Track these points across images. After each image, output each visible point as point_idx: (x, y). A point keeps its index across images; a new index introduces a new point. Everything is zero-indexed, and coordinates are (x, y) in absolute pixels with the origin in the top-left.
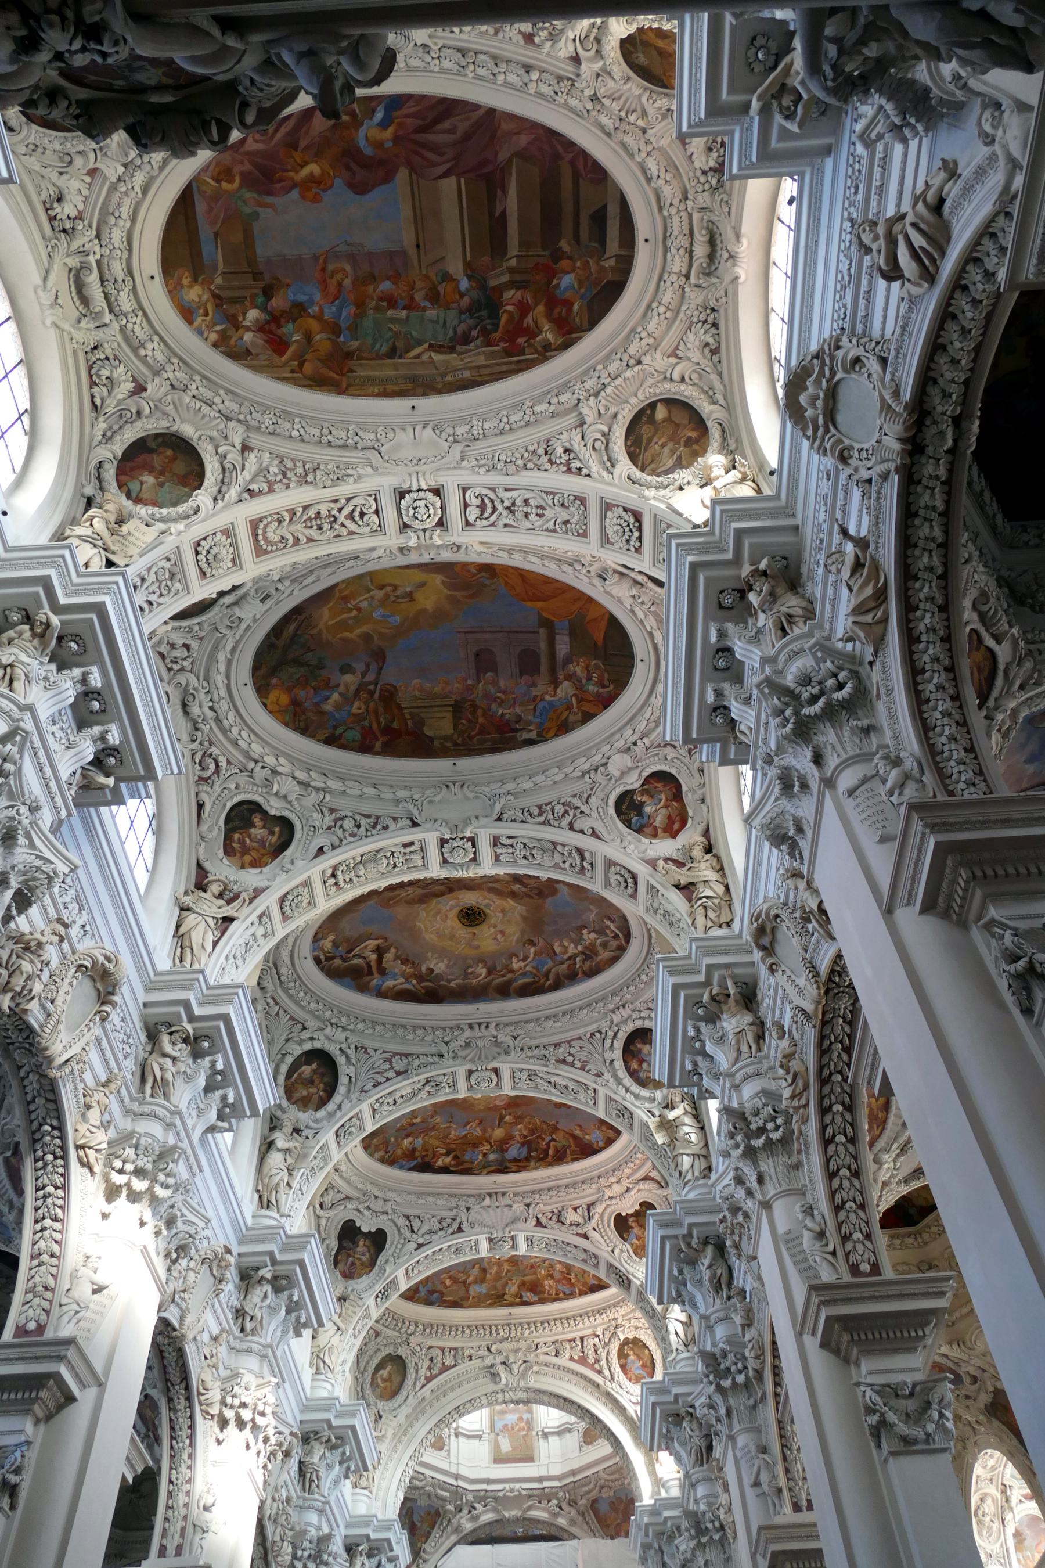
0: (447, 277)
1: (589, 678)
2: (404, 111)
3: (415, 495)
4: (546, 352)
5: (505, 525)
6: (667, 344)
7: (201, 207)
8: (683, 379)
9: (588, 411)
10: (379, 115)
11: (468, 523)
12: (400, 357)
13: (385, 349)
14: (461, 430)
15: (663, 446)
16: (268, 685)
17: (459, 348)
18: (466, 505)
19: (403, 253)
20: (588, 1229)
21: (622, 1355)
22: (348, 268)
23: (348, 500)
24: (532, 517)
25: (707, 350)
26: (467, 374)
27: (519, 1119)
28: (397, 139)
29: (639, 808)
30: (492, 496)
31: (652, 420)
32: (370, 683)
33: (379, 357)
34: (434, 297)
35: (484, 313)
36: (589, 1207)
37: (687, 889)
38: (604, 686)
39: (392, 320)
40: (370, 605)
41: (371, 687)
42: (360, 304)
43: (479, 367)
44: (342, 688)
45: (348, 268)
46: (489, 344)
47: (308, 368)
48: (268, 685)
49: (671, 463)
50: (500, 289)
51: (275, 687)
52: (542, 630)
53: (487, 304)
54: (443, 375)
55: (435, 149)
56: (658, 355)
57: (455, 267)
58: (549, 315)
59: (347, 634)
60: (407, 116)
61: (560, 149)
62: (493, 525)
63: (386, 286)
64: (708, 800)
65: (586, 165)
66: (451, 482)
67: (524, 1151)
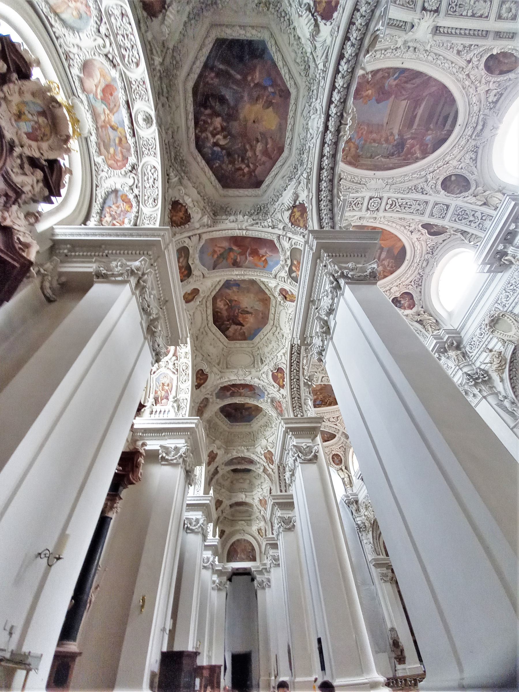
0: (392, 134)
1: (388, 265)
3: (375, 199)
4: (417, 160)
5: (397, 211)
6: (458, 158)
8: (462, 168)
9: (429, 177)
11: (385, 210)
12: (373, 158)
13: (369, 155)
14: (390, 181)
15: (455, 187)
17: (390, 157)
18: (387, 204)
19: (382, 125)
20: (337, 423)
21: (333, 458)
22: (366, 128)
23: (357, 198)
24: (406, 208)
25: (471, 160)
26: (391, 165)
27: (321, 393)
28: (396, 85)
29: (400, 302)
30: (396, 201)
31: (450, 180)
33: (367, 158)
34: (387, 140)
35: (400, 147)
36: (337, 417)
37: (420, 322)
38: (392, 268)
39: (372, 147)
42: (366, 141)
43: (395, 164)
45: (366, 128)
46: (399, 156)
47: (348, 158)
49: (458, 192)
50: (407, 140)
52: (379, 250)
53: (401, 145)
54: (384, 165)
56: (455, 161)
57: (396, 131)
58: (420, 149)
62: (393, 211)
63: (374, 135)
64: (423, 299)
66: (385, 195)
67: (321, 402)
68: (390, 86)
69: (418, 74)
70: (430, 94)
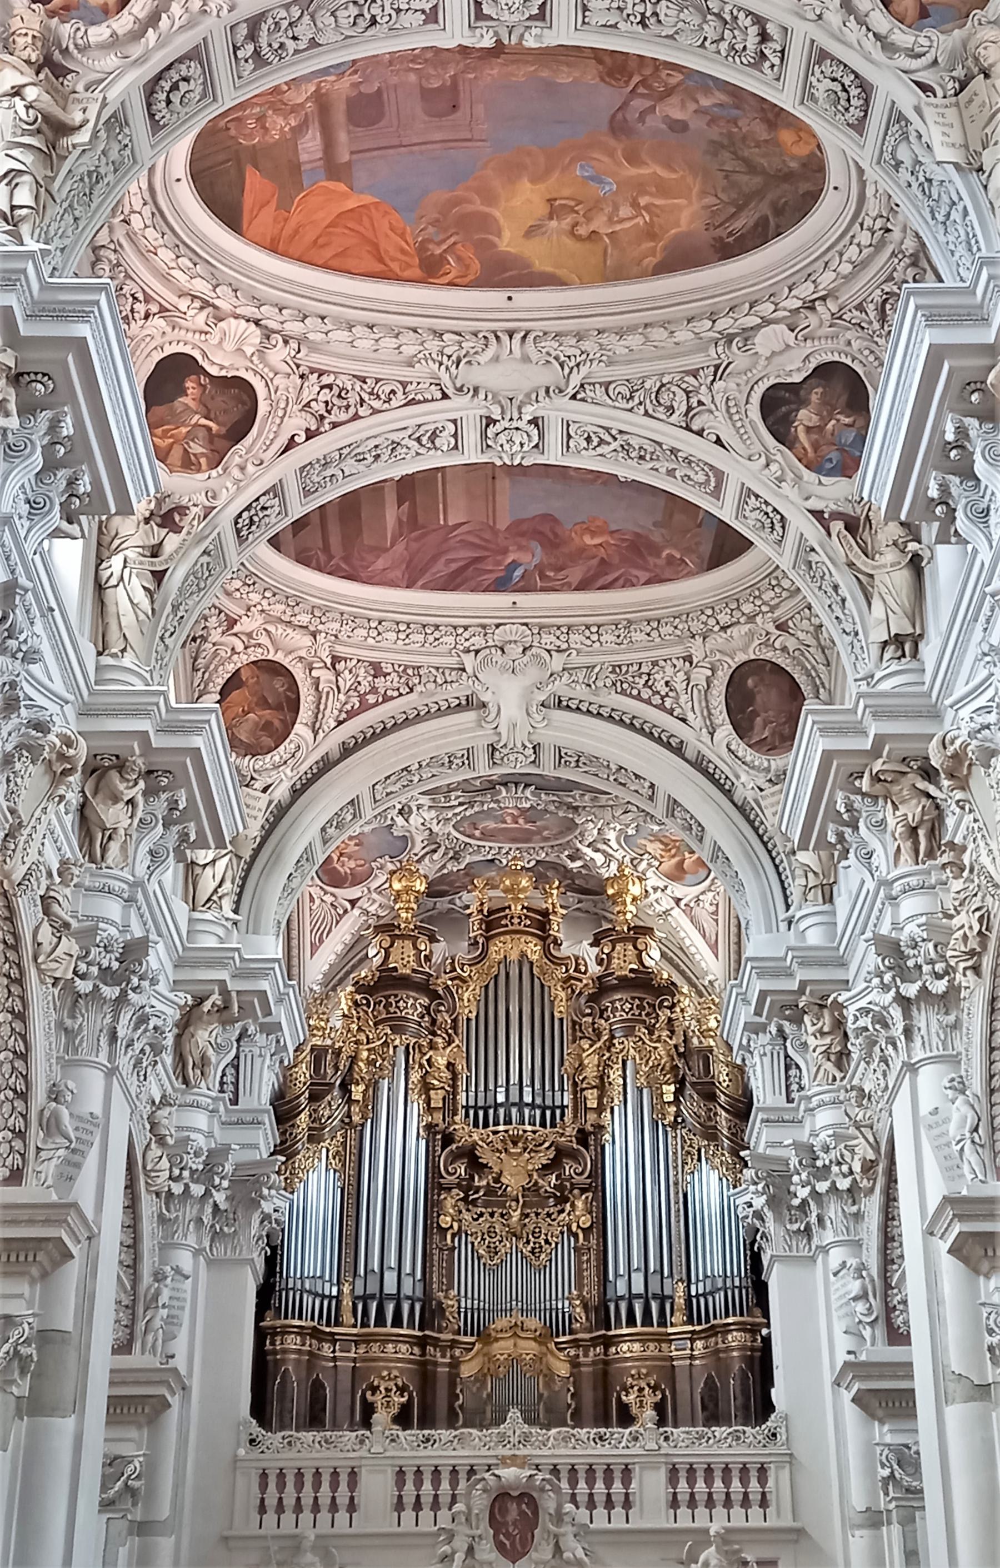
2: (493, 576)
7: (706, 548)
10: (518, 573)
11: (454, 422)
16: (804, 165)
28: (505, 552)
32: (643, 96)
40: (616, 208)
41: (641, 90)
44: (692, 106)
48: (804, 165)
51: (793, 158)
55: (465, 544)
59: (661, 172)
60: (491, 571)
61: (344, 566)
65: (318, 561)
68: (521, 548)
69: (450, 584)
70: (386, 550)
